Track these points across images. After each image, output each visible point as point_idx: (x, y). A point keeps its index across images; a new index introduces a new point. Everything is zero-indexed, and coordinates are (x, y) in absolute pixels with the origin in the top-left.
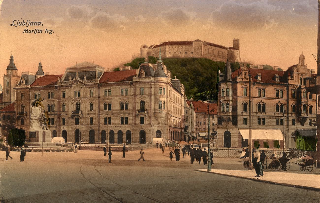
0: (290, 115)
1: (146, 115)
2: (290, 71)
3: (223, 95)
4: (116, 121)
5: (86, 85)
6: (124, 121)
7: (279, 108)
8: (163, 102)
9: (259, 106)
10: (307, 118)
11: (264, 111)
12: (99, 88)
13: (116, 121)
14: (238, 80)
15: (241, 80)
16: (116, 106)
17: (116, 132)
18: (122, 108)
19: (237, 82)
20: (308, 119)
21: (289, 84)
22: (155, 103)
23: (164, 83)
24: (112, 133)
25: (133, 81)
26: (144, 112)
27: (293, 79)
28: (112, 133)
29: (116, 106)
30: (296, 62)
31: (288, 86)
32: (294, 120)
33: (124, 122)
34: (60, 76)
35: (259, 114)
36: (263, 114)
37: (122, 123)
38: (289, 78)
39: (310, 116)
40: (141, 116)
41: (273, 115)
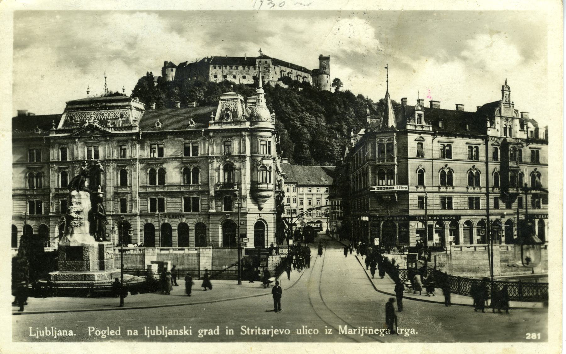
0: (490, 189)
1: (237, 192)
4: (174, 205)
6: (192, 205)
7: (473, 179)
8: (268, 168)
9: (443, 175)
11: (450, 183)
13: (174, 205)
15: (414, 128)
16: (174, 175)
17: (175, 227)
19: (406, 132)
21: (488, 136)
22: (252, 170)
23: (270, 131)
25: (210, 128)
26: (234, 188)
28: (166, 228)
29: (174, 175)
30: (497, 97)
31: (486, 138)
32: (496, 199)
33: (157, 207)
34: (57, 118)
35: (443, 189)
36: (450, 189)
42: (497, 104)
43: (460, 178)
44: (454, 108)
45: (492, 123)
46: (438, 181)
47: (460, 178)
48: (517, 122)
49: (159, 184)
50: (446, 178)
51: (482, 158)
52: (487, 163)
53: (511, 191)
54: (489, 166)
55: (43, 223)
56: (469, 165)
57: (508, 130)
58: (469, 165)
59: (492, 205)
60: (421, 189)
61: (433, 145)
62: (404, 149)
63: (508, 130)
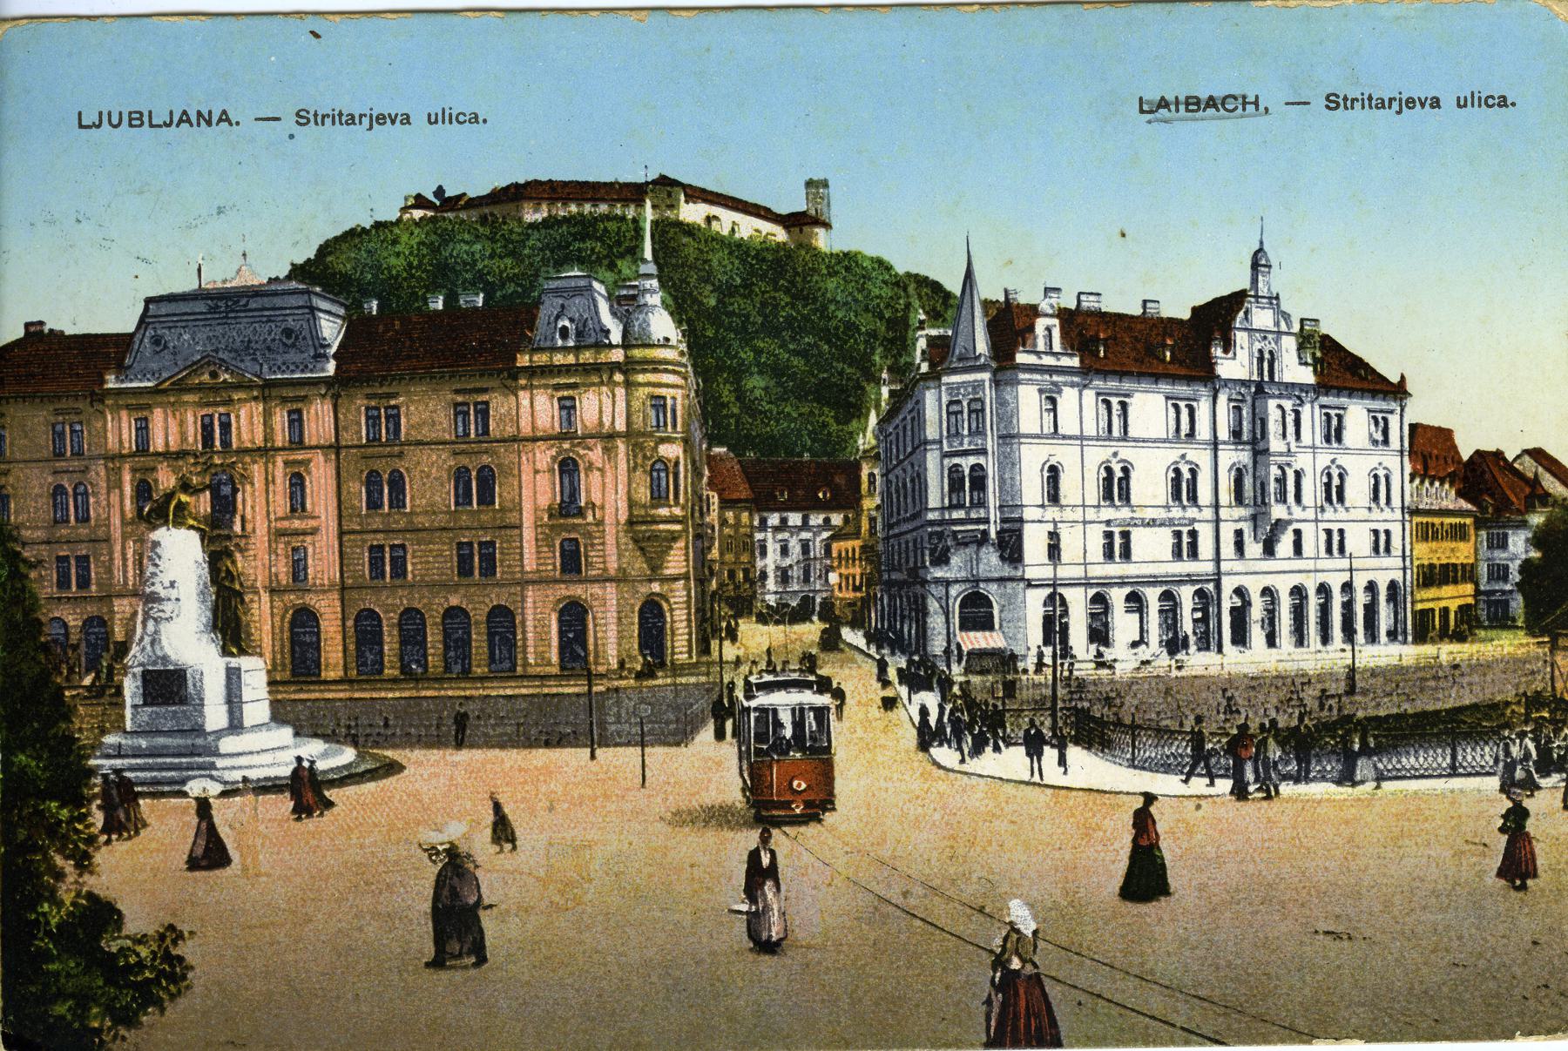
0: (1223, 513)
2: (1217, 318)
3: (953, 430)
5: (270, 384)
7: (1182, 487)
10: (1289, 522)
12: (336, 398)
14: (1021, 358)
18: (463, 498)
20: (1291, 528)
23: (674, 372)
24: (412, 623)
27: (1230, 355)
28: (412, 623)
30: (1237, 279)
35: (1108, 513)
36: (1125, 513)
37: (465, 569)
38: (1217, 352)
39: (1297, 512)
40: (565, 535)
41: (1161, 514)
42: (1236, 301)
43: (1150, 487)
44: (1136, 311)
45: (1228, 346)
46: (1093, 494)
47: (1150, 487)
48: (1289, 344)
49: (391, 507)
50: (1116, 486)
51: (1203, 431)
52: (1215, 444)
53: (1278, 511)
54: (1220, 453)
55: (92, 609)
56: (1171, 455)
57: (1266, 361)
58: (1171, 455)
59: (1228, 549)
60: (1052, 513)
61: (1079, 407)
62: (1007, 415)
63: (1266, 361)
